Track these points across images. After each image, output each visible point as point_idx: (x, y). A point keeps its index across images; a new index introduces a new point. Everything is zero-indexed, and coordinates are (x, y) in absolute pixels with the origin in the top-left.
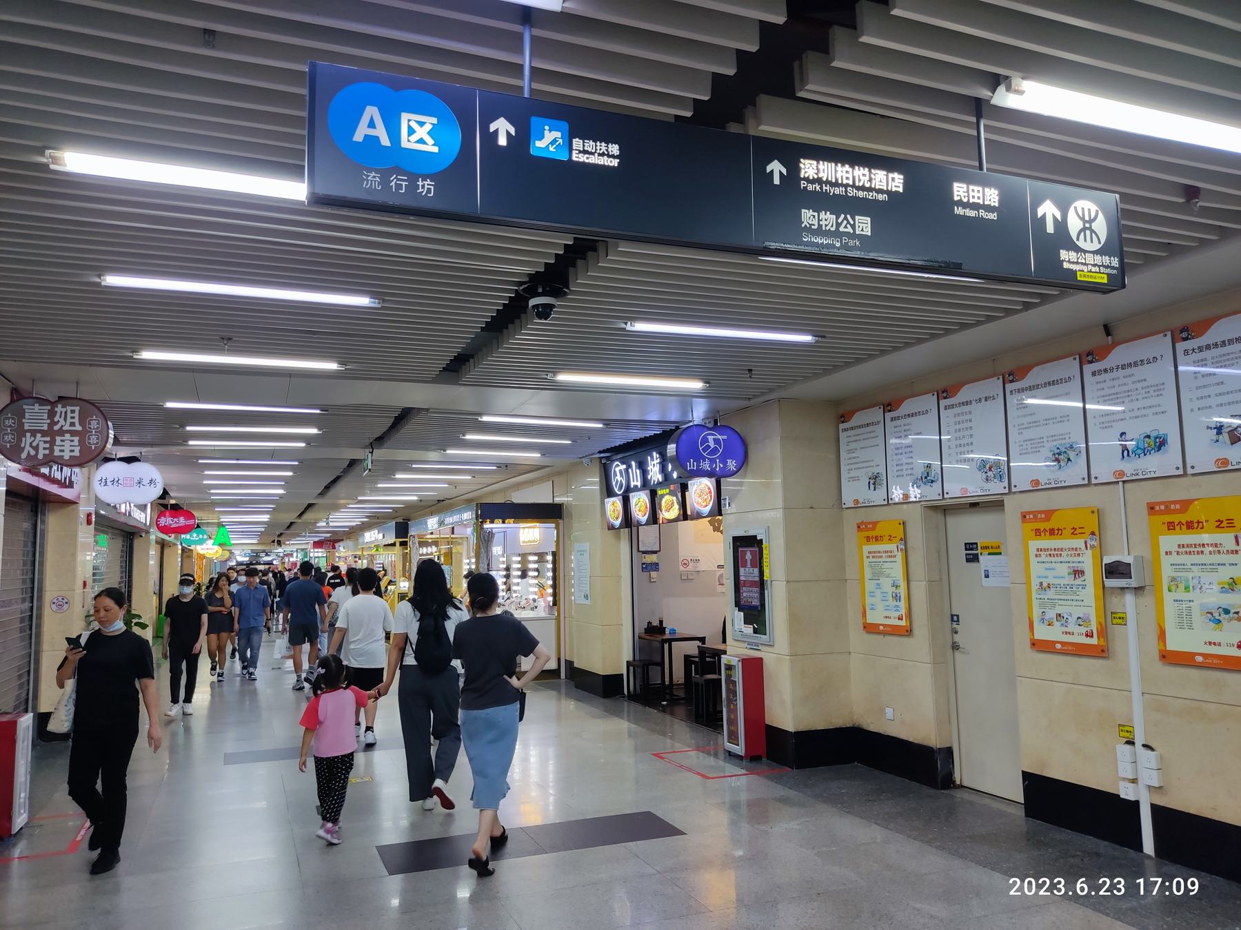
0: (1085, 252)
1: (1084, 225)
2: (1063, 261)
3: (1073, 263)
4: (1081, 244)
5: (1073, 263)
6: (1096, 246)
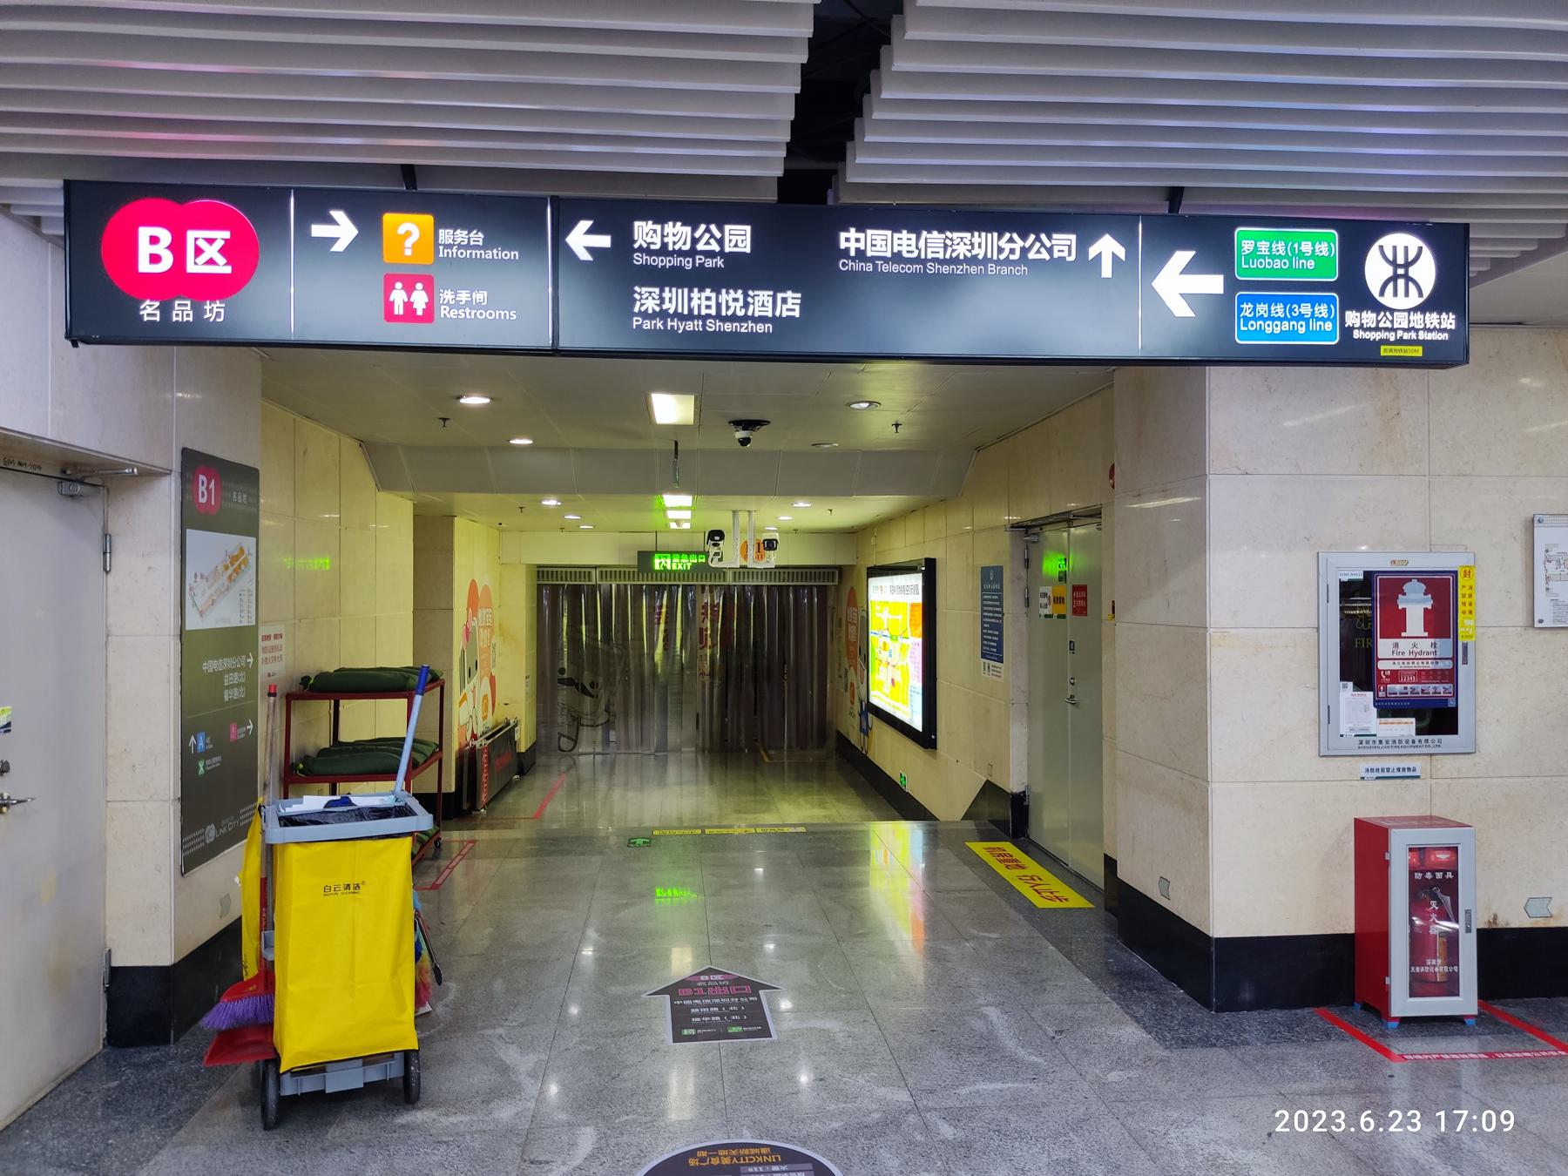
0: (1392, 311)
1: (1395, 272)
3: (1370, 329)
4: (1387, 300)
5: (1370, 329)
6: (1415, 300)
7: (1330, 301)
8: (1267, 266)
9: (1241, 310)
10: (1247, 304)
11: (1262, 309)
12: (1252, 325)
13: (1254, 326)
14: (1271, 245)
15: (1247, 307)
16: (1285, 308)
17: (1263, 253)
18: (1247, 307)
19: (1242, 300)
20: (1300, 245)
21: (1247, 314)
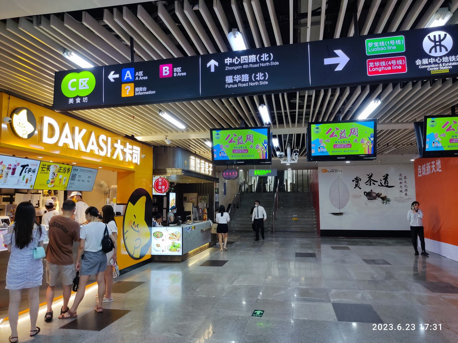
2: (419, 65)
7: (404, 58)
8: (378, 50)
9: (369, 65)
10: (371, 63)
11: (377, 64)
12: (374, 69)
13: (374, 70)
14: (379, 43)
15: (371, 64)
16: (386, 63)
17: (376, 46)
18: (371, 64)
19: (369, 62)
20: (390, 42)
21: (371, 66)
